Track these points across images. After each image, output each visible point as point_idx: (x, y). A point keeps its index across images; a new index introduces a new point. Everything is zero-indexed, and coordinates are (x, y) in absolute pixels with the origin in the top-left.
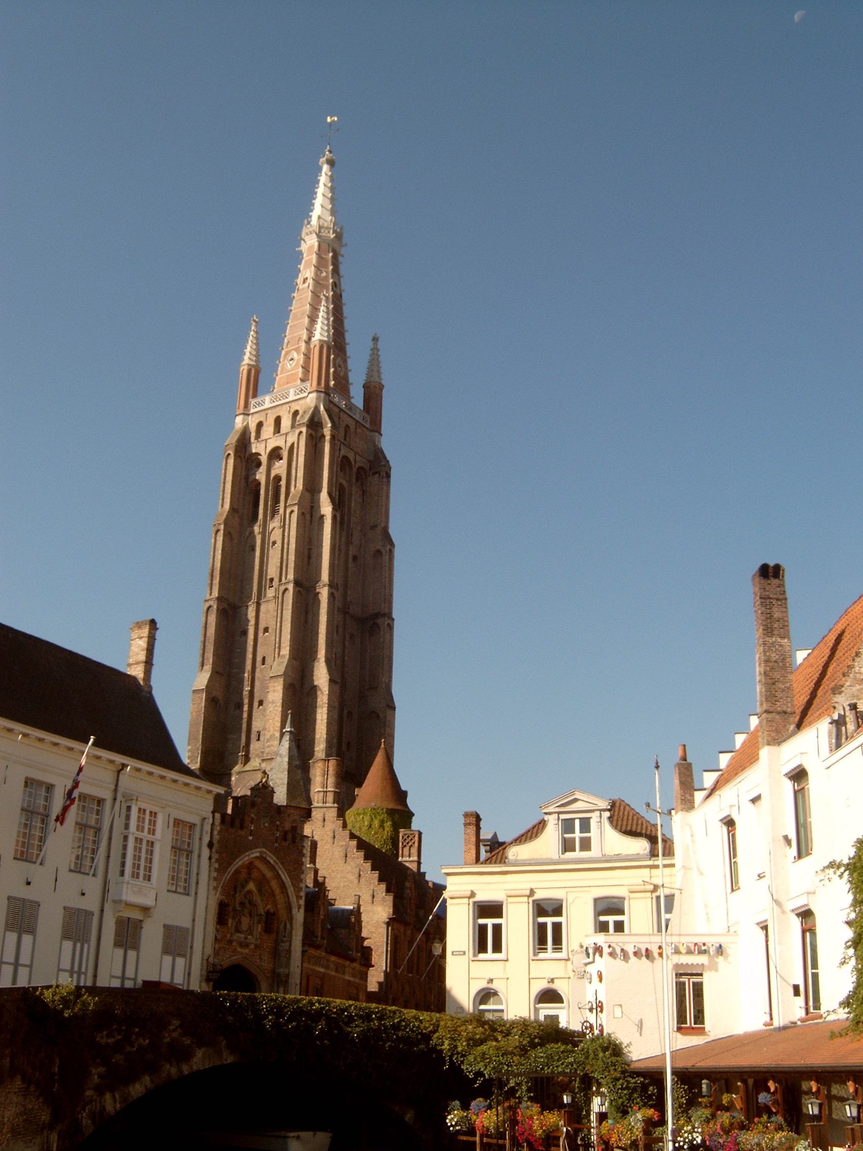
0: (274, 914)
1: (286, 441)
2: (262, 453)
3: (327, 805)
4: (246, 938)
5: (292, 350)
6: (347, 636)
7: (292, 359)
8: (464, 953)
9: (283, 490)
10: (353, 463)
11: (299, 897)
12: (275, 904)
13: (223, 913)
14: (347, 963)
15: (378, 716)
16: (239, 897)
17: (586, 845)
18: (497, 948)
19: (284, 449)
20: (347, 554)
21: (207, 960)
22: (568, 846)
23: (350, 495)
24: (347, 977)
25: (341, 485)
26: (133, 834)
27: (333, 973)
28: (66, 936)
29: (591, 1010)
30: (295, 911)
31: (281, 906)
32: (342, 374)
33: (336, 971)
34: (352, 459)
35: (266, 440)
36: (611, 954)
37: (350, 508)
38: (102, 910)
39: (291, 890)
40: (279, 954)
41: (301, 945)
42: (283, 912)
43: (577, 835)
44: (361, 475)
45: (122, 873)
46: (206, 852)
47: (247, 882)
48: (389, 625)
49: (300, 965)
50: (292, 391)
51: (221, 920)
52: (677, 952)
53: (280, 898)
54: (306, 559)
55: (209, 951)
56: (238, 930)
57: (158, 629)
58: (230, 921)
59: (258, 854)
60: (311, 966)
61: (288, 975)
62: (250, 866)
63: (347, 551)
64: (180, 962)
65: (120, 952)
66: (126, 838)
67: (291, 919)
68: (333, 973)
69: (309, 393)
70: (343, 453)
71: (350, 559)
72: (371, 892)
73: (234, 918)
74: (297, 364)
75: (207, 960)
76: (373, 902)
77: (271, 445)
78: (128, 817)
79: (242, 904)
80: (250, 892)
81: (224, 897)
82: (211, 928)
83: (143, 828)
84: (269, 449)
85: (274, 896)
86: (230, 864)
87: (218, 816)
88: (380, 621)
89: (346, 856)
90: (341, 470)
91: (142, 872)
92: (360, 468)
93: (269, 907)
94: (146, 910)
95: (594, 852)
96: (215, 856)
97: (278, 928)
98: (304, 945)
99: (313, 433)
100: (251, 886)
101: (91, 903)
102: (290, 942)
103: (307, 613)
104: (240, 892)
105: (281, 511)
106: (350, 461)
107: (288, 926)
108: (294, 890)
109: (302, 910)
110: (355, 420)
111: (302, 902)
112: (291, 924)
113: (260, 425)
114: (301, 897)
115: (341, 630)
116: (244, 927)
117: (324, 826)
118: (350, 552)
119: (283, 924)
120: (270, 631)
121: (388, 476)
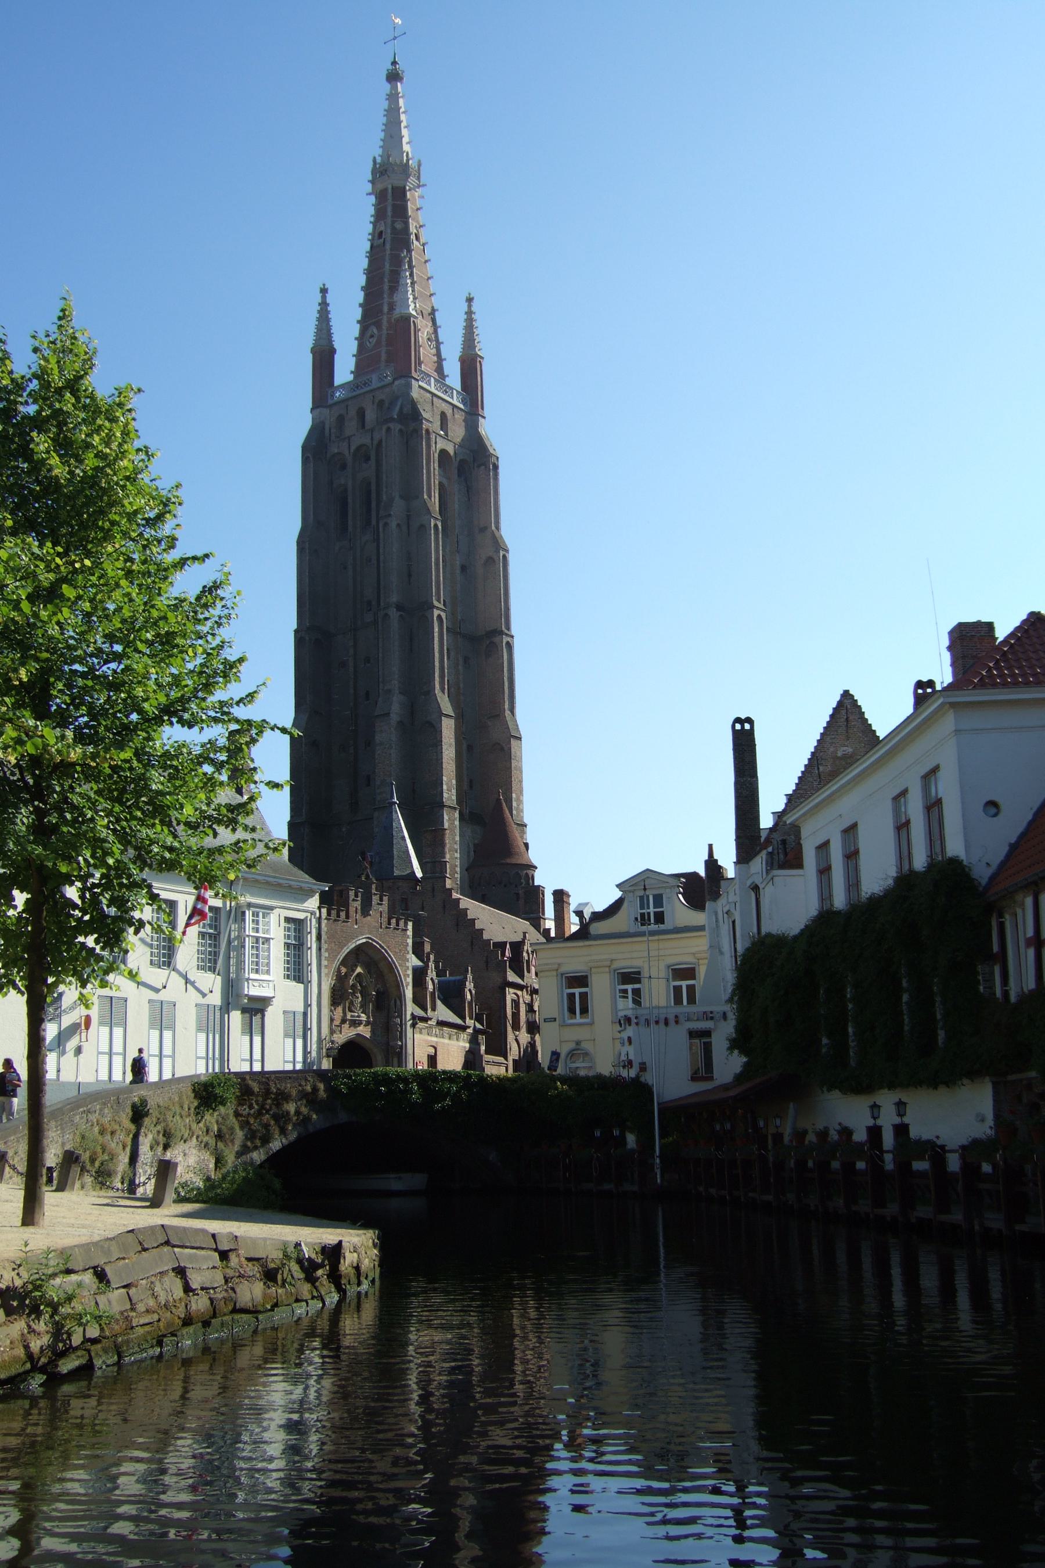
2: (346, 453)
5: (370, 324)
8: (555, 1020)
9: (374, 495)
15: (502, 749)
29: (624, 1067)
35: (349, 438)
36: (637, 1024)
48: (508, 643)
52: (689, 1020)
59: (364, 940)
70: (439, 446)
71: (458, 571)
72: (485, 959)
74: (378, 343)
77: (356, 442)
84: (353, 448)
88: (496, 640)
89: (457, 925)
93: (378, 986)
95: (668, 924)
99: (403, 428)
105: (374, 522)
107: (398, 1002)
111: (410, 980)
112: (401, 1002)
113: (341, 420)
114: (408, 976)
119: (393, 1001)
121: (496, 467)
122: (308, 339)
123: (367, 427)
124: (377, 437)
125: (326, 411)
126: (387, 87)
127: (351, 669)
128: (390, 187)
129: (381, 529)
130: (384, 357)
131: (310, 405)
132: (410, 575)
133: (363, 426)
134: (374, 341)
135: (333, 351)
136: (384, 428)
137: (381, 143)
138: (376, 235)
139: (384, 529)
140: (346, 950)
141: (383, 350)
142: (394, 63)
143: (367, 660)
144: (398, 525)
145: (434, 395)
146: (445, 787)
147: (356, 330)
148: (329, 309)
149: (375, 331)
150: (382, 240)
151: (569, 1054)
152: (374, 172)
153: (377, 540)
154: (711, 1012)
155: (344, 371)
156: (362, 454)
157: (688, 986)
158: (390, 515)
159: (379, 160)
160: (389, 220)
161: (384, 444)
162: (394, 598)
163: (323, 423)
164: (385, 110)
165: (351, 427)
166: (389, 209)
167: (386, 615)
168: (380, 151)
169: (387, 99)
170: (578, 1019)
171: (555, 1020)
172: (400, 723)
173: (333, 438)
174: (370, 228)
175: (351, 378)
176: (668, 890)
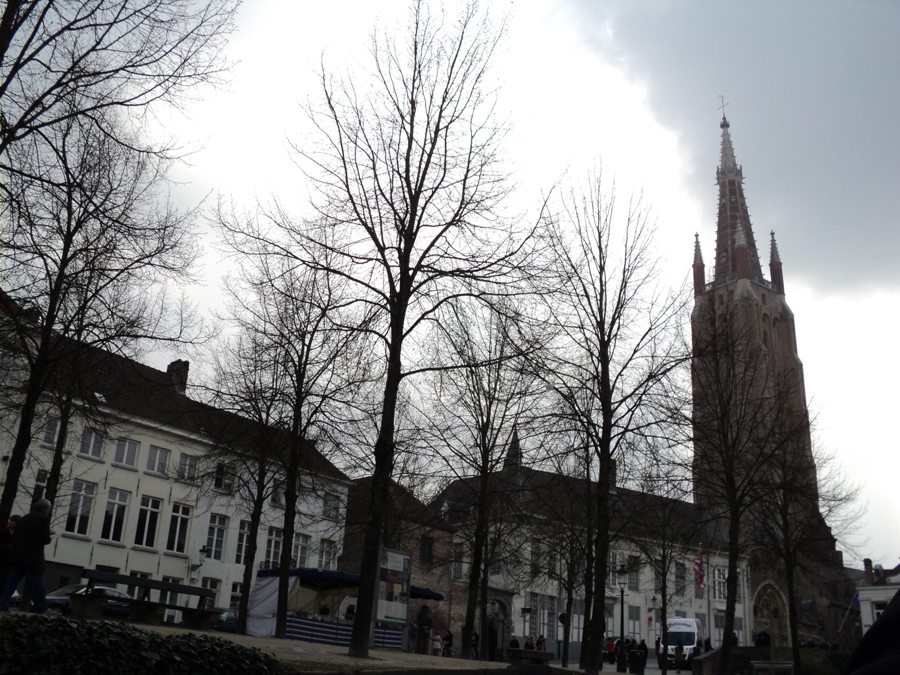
13: (756, 610)
32: (755, 261)
40: (781, 627)
45: (715, 597)
46: (746, 585)
51: (755, 613)
53: (779, 601)
55: (752, 627)
56: (762, 617)
62: (765, 588)
79: (763, 605)
80: (766, 600)
86: (756, 589)
87: (749, 568)
96: (750, 585)
101: (704, 611)
125: (701, 297)
126: (721, 131)
130: (730, 268)
134: (724, 259)
135: (703, 266)
140: (759, 588)
141: (730, 264)
142: (724, 118)
145: (758, 286)
147: (714, 254)
149: (725, 254)
152: (718, 173)
155: (709, 275)
160: (728, 198)
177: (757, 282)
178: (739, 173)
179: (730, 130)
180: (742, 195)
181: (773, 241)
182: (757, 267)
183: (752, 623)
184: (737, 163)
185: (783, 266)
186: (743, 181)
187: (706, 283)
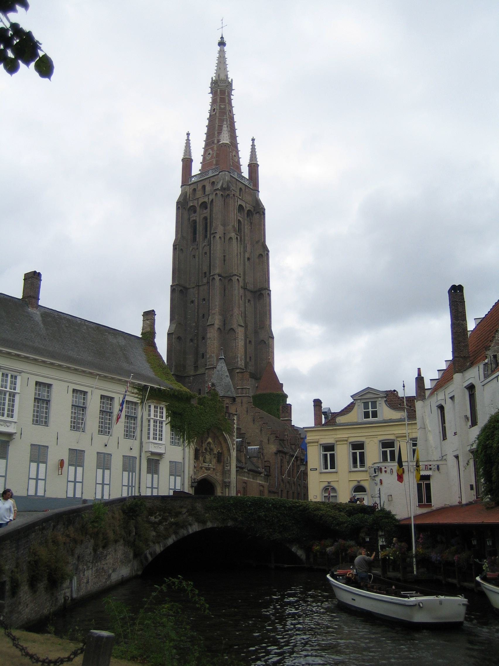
0: (221, 453)
1: (208, 199)
3: (244, 395)
4: (209, 465)
6: (247, 301)
7: (209, 154)
9: (208, 225)
10: (245, 208)
11: (233, 444)
12: (222, 448)
14: (258, 474)
15: (265, 343)
16: (204, 445)
17: (375, 415)
18: (333, 466)
19: (208, 202)
20: (244, 257)
21: (191, 477)
22: (366, 415)
23: (244, 225)
24: (258, 482)
25: (239, 221)
26: (152, 419)
27: (252, 480)
28: (124, 470)
30: (231, 451)
31: (225, 449)
32: (236, 160)
33: (253, 479)
34: (244, 206)
37: (244, 233)
38: (141, 456)
39: (229, 441)
40: (226, 473)
41: (235, 467)
42: (225, 452)
43: (370, 410)
44: (250, 213)
45: (149, 438)
47: (207, 438)
48: (268, 294)
49: (236, 478)
50: (210, 171)
51: (196, 457)
53: (224, 445)
54: (223, 262)
55: (192, 473)
56: (204, 462)
57: (156, 315)
58: (200, 458)
60: (241, 477)
61: (230, 482)
63: (244, 255)
64: (178, 479)
65: (150, 476)
66: (149, 421)
67: (230, 455)
68: (252, 480)
69: (219, 172)
70: (239, 203)
71: (246, 260)
72: (267, 438)
73: (202, 456)
74: (212, 157)
75: (191, 477)
76: (269, 443)
77: (201, 201)
78: (150, 411)
79: (206, 449)
80: (209, 443)
81: (197, 446)
82: (192, 461)
83: (157, 415)
84: (200, 203)
85: (221, 444)
88: (263, 292)
89: (254, 420)
90: (239, 212)
91: (158, 437)
92: (249, 210)
93: (219, 449)
94: (160, 455)
97: (224, 460)
98: (237, 467)
99: (223, 193)
100: (210, 440)
101: (135, 453)
102: (230, 466)
103: (225, 290)
104: (205, 443)
105: (208, 236)
106: (243, 207)
107: (229, 458)
108: (231, 441)
109: (235, 450)
110: (245, 185)
111: (235, 446)
112: (230, 458)
113: (194, 190)
114: (234, 444)
115: (243, 298)
116: (207, 460)
117: (242, 406)
118: (246, 256)
119: (226, 458)
120: (206, 300)
121: (264, 214)
122: (181, 155)
123: (207, 193)
124: (211, 198)
126: (218, 48)
127: (196, 304)
128: (219, 90)
129: (212, 239)
131: (181, 185)
132: (224, 261)
133: (204, 193)
135: (191, 161)
136: (214, 193)
137: (215, 72)
138: (212, 110)
139: (213, 240)
142: (222, 38)
143: (204, 300)
144: (220, 237)
145: (237, 180)
146: (239, 359)
147: (202, 152)
148: (190, 142)
150: (215, 113)
151: (324, 488)
152: (212, 83)
153: (210, 245)
154: (430, 465)
155: (196, 169)
156: (204, 205)
157: (390, 451)
158: (216, 233)
159: (214, 79)
160: (218, 104)
161: (214, 201)
162: (217, 271)
163: (186, 192)
164: (218, 51)
165: (199, 193)
166: (218, 100)
167: (214, 279)
168: (215, 75)
169: (218, 53)
170: (329, 470)
171: (316, 469)
172: (219, 328)
173: (191, 199)
174: (209, 108)
175: (200, 172)
176: (380, 399)
177: (236, 177)
178: (230, 85)
179: (226, 48)
180: (230, 103)
181: (253, 146)
182: (238, 166)
183: (192, 467)
184: (229, 77)
185: (259, 168)
186: (233, 92)
187: (193, 174)
